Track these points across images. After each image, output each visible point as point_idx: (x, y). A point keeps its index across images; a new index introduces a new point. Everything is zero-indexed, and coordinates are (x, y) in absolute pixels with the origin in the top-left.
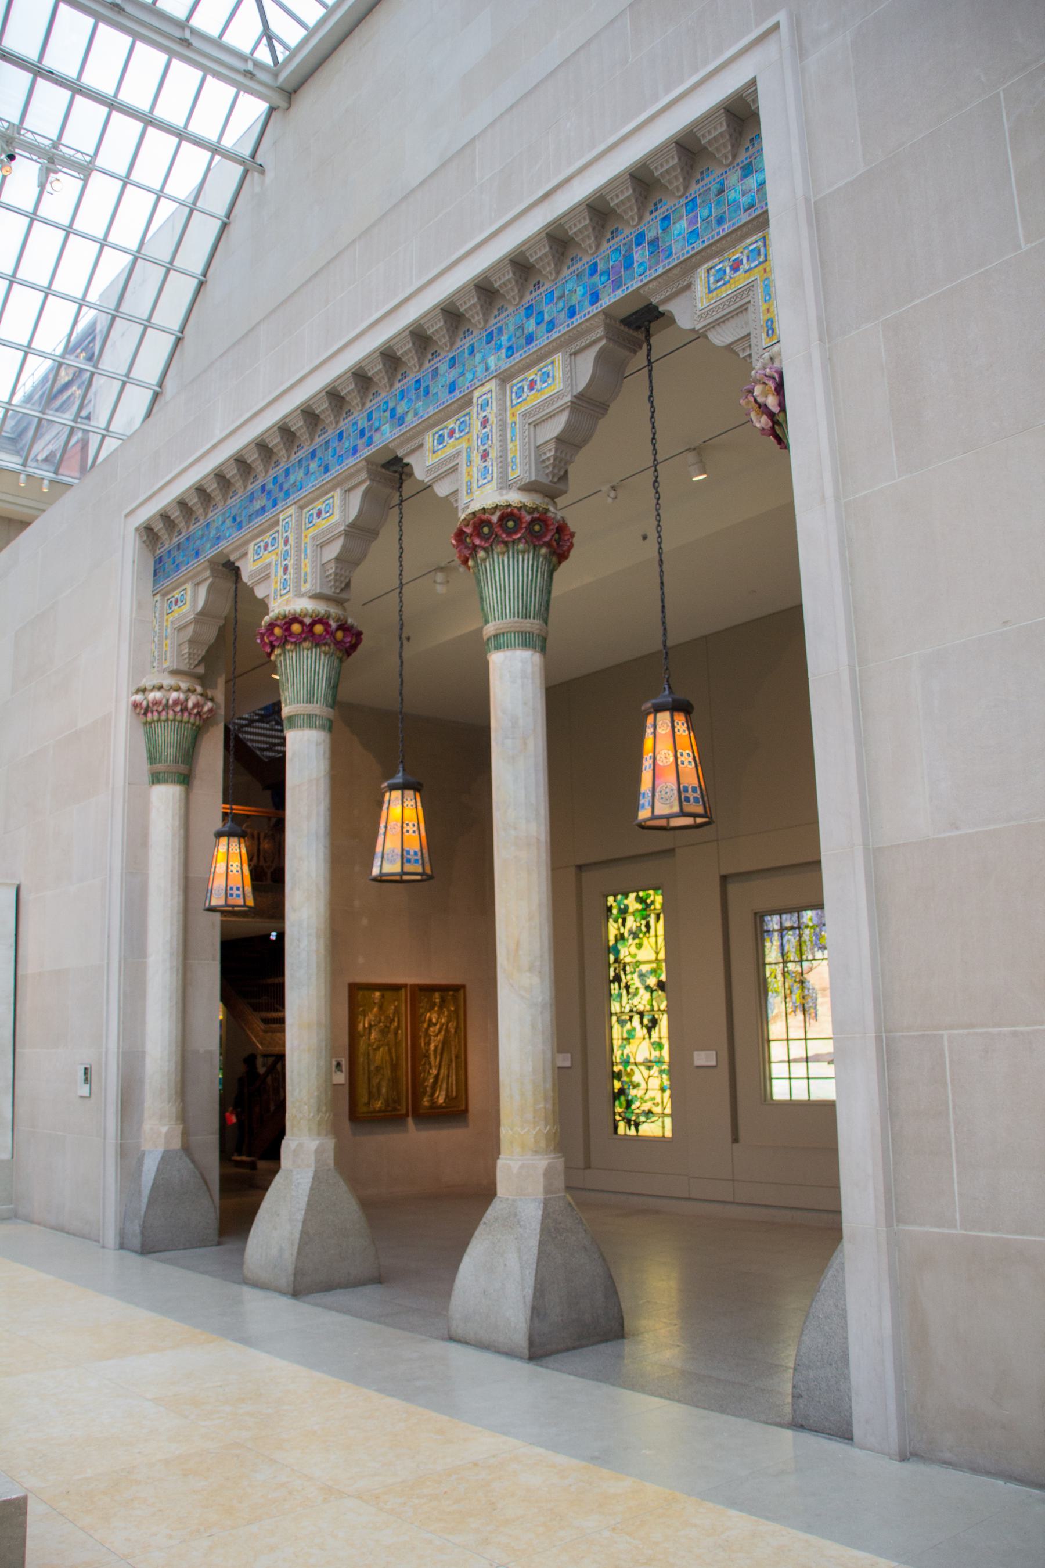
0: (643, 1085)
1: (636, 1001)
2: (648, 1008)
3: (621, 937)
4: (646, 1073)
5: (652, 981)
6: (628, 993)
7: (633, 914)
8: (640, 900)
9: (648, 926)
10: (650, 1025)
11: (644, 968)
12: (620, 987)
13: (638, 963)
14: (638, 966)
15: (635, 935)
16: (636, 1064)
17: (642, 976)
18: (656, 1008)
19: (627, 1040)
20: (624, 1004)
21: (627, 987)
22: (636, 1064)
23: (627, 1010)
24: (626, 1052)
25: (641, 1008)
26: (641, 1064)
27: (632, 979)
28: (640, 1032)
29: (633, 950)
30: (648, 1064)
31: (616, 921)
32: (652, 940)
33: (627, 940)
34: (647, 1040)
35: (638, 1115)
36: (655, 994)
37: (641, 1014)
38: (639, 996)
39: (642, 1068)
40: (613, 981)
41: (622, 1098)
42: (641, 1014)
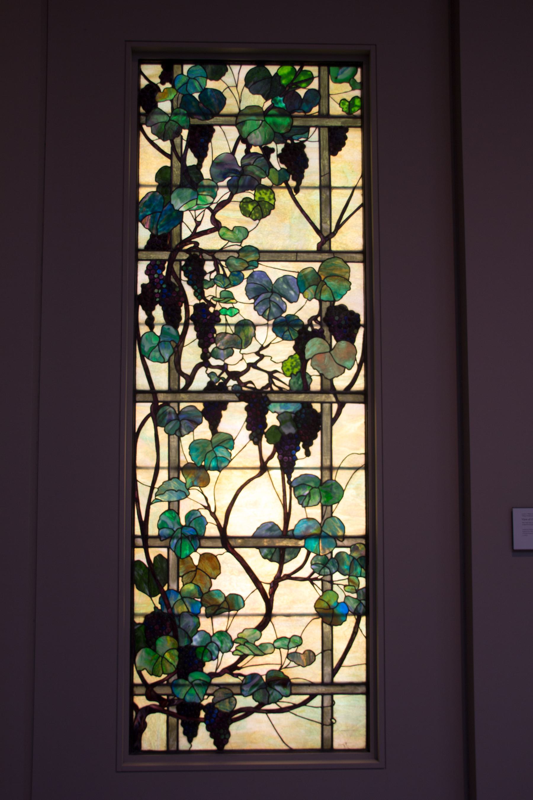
10: (289, 430)
20: (187, 367)
27: (229, 298)
33: (212, 190)
34: (277, 475)
38: (254, 346)
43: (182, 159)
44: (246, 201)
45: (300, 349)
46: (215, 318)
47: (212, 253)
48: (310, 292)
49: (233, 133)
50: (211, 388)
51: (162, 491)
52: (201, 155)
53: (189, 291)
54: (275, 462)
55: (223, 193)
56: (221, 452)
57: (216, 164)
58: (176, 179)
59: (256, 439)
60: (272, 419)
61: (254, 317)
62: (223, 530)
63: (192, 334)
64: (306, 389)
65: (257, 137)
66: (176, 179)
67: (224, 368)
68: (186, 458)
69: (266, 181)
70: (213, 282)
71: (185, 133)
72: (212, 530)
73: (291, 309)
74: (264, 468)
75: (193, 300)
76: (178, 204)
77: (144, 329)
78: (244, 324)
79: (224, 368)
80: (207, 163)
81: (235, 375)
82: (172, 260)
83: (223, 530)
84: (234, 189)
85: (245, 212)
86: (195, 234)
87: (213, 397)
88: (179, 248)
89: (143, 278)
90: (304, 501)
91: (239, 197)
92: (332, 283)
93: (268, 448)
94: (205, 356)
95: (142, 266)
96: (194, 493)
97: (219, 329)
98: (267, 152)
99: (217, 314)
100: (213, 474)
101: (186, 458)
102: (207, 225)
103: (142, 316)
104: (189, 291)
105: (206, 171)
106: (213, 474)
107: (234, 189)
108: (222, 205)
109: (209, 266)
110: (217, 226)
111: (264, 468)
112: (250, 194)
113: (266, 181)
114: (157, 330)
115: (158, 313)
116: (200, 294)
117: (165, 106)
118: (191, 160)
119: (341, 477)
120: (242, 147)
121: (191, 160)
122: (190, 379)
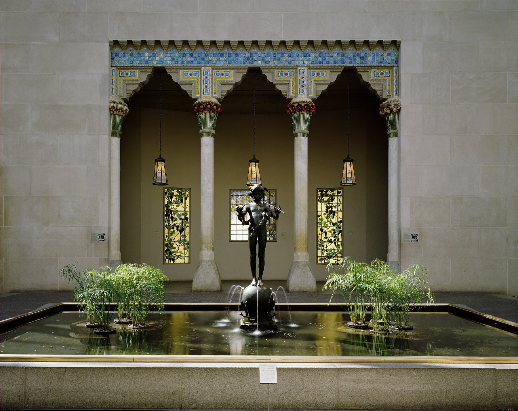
0: (177, 248)
1: (175, 223)
2: (180, 225)
3: (169, 203)
4: (178, 244)
5: (183, 217)
6: (172, 220)
7: (176, 196)
8: (178, 191)
9: (182, 201)
10: (181, 230)
11: (179, 213)
12: (169, 218)
13: (177, 211)
14: (177, 212)
15: (176, 202)
16: (174, 241)
17: (179, 215)
18: (184, 225)
19: (171, 234)
20: (170, 223)
21: (172, 218)
22: (174, 241)
23: (172, 225)
24: (170, 238)
25: (178, 225)
26: (176, 241)
27: (175, 216)
28: (176, 232)
29: (175, 207)
30: (179, 242)
31: (168, 197)
32: (183, 205)
33: (173, 204)
34: (180, 235)
35: (175, 257)
36: (183, 221)
37: (178, 227)
38: (177, 221)
39: (177, 243)
40: (166, 216)
41: (168, 252)
42: (178, 227)
43: (170, 200)
44: (177, 205)
45: (182, 221)
46: (173, 218)
47: (173, 211)
48: (183, 215)
49: (175, 197)
50: (173, 225)
51: (168, 236)
52: (172, 200)
53: (170, 215)
54: (179, 233)
55: (174, 204)
56: (174, 232)
57: (173, 201)
58: (169, 202)
59: (177, 231)
60: (179, 229)
61: (177, 218)
62: (174, 240)
63: (171, 219)
64: (183, 226)
65: (178, 198)
66: (169, 202)
67: (174, 223)
68: (170, 233)
69: (179, 203)
70: (173, 214)
71: (170, 197)
72: (173, 240)
73: (181, 217)
74: (178, 234)
75: (171, 216)
76: (169, 205)
77: (166, 219)
78: (176, 219)
79: (174, 223)
80: (172, 201)
81: (175, 224)
82: (169, 211)
83: (174, 240)
84: (175, 204)
85: (176, 206)
86: (171, 209)
87: (173, 226)
88: (169, 210)
89: (165, 213)
90: (182, 237)
91: (176, 205)
92: (186, 214)
93: (179, 232)
94: (172, 222)
95: (165, 212)
96: (171, 236)
97: (174, 219)
98: (179, 200)
99: (173, 217)
100: (173, 234)
101: (170, 233)
102: (172, 208)
103: (165, 217)
104: (170, 215)
105: (172, 202)
106: (173, 234)
107: (175, 204)
108: (174, 205)
109: (172, 212)
110: (173, 208)
111: (178, 234)
112: (177, 204)
113: (179, 203)
114: (167, 219)
115: (167, 217)
116: (172, 215)
117: (168, 194)
118: (171, 200)
119: (186, 235)
120: (176, 199)
121: (171, 200)
122: (171, 224)
